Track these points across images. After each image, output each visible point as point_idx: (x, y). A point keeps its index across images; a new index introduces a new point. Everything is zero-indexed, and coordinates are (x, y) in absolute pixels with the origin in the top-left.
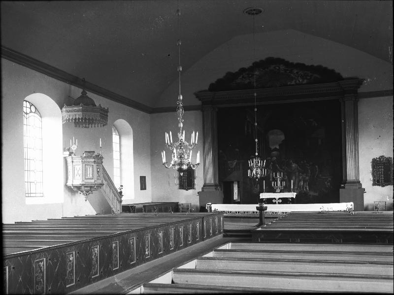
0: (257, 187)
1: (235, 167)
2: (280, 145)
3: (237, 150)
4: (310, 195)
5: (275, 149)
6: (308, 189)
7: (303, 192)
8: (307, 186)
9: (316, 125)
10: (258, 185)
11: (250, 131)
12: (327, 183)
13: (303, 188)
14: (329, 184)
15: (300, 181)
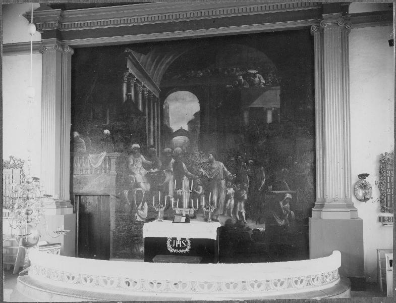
0: (142, 209)
1: (101, 166)
2: (190, 123)
3: (107, 131)
4: (248, 229)
5: (181, 132)
6: (244, 214)
7: (234, 222)
8: (243, 211)
9: (264, 81)
10: (146, 205)
11: (133, 94)
12: (284, 204)
13: (234, 212)
14: (287, 205)
15: (228, 197)
